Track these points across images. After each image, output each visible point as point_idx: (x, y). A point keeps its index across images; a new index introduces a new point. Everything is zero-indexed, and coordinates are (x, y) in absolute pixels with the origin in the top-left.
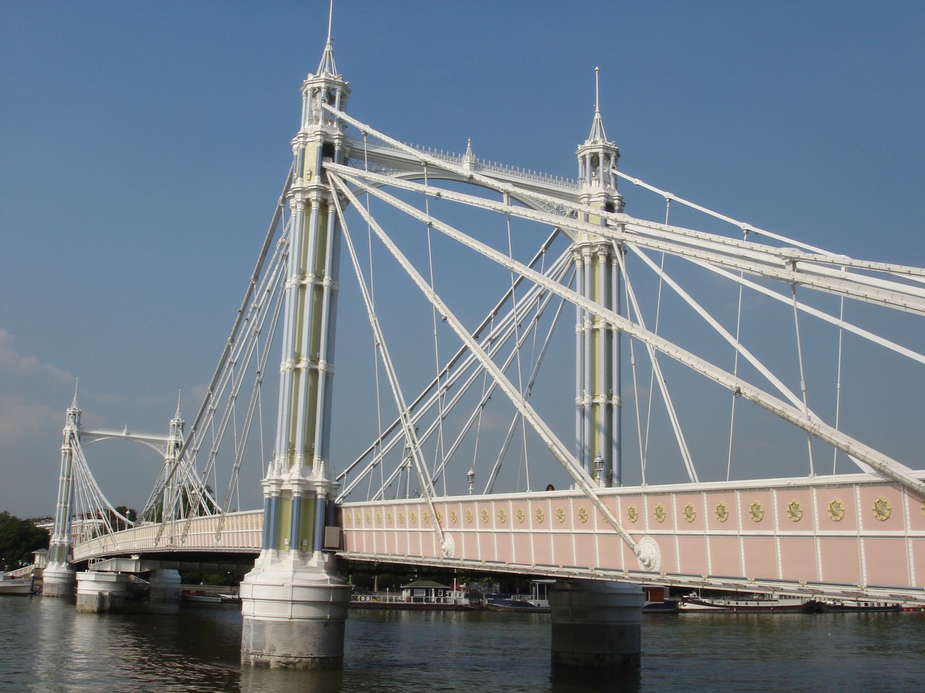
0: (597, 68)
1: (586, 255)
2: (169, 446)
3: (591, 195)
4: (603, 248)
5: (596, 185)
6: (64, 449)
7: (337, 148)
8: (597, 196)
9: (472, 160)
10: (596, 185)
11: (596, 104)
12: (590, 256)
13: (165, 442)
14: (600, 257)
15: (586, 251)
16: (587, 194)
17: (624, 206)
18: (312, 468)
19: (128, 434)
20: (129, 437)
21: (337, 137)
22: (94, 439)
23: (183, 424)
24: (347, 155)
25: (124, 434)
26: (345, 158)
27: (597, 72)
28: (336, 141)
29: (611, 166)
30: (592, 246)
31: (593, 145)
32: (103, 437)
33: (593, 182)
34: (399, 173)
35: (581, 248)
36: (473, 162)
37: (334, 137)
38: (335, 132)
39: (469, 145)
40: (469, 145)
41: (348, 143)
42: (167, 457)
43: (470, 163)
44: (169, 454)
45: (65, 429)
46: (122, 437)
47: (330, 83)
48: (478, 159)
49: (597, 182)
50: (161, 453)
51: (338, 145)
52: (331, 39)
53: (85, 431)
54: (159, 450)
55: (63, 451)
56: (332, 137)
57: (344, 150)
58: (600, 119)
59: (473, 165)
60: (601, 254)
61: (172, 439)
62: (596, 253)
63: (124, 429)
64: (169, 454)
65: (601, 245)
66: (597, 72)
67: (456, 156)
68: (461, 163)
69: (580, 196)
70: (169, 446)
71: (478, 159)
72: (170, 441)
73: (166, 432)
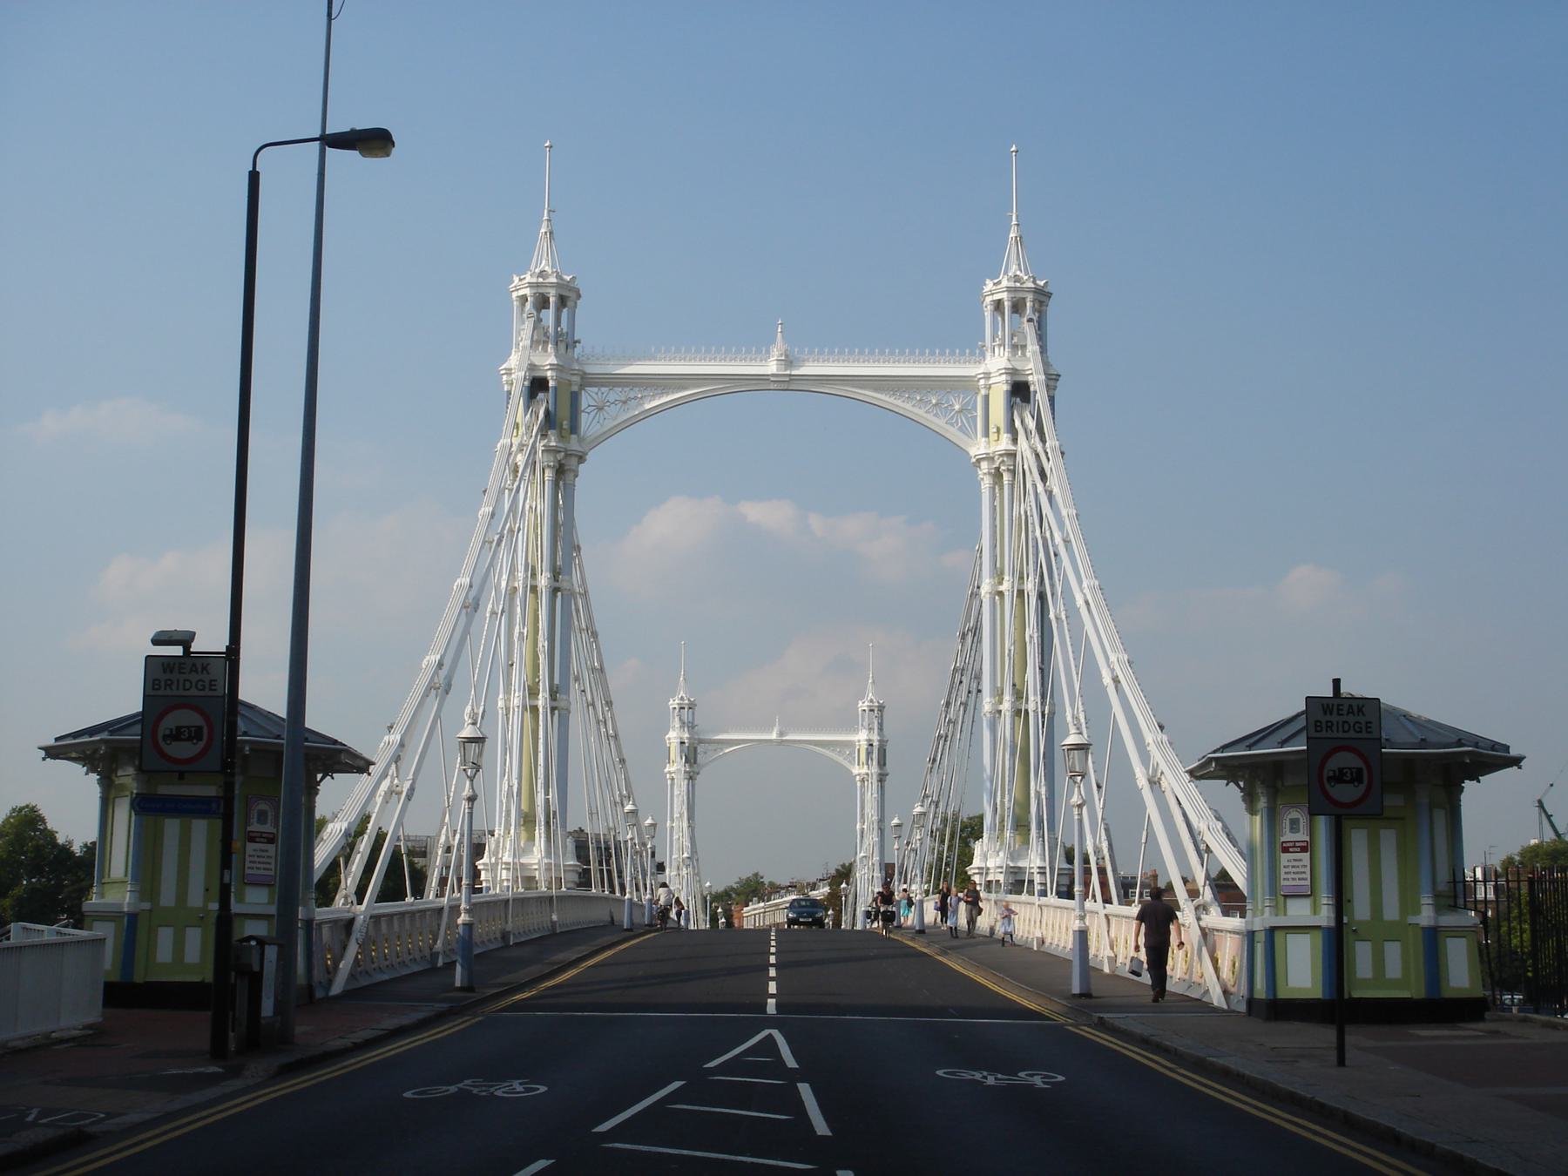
0: (1014, 148)
1: (985, 474)
2: (859, 750)
3: (990, 373)
4: (1005, 459)
5: (999, 355)
6: (670, 773)
7: (551, 384)
8: (997, 374)
9: (781, 355)
10: (999, 355)
11: (1012, 212)
12: (989, 473)
13: (850, 744)
14: (1004, 474)
15: (984, 465)
16: (983, 373)
17: (1058, 380)
18: (534, 845)
19: (781, 734)
20: (783, 741)
21: (548, 367)
22: (722, 749)
23: (881, 708)
24: (575, 388)
25: (774, 736)
26: (572, 393)
27: (1014, 154)
28: (549, 374)
29: (1025, 319)
30: (990, 459)
31: (994, 288)
32: (737, 745)
33: (996, 349)
34: (665, 395)
35: (979, 461)
36: (783, 358)
37: (546, 368)
38: (547, 360)
39: (779, 330)
40: (779, 330)
41: (572, 370)
42: (856, 770)
43: (777, 360)
44: (859, 764)
45: (667, 736)
46: (770, 741)
47: (538, 286)
48: (796, 350)
49: (1002, 348)
50: (846, 763)
51: (552, 379)
52: (549, 211)
53: (701, 737)
54: (840, 759)
55: (668, 776)
56: (542, 368)
57: (570, 381)
58: (1016, 237)
59: (783, 363)
60: (1004, 470)
61: (861, 737)
62: (999, 468)
63: (775, 725)
64: (859, 764)
65: (1001, 455)
66: (1014, 154)
67: (759, 351)
68: (766, 361)
69: (975, 377)
70: (859, 750)
71: (796, 350)
72: (859, 741)
73: (852, 726)
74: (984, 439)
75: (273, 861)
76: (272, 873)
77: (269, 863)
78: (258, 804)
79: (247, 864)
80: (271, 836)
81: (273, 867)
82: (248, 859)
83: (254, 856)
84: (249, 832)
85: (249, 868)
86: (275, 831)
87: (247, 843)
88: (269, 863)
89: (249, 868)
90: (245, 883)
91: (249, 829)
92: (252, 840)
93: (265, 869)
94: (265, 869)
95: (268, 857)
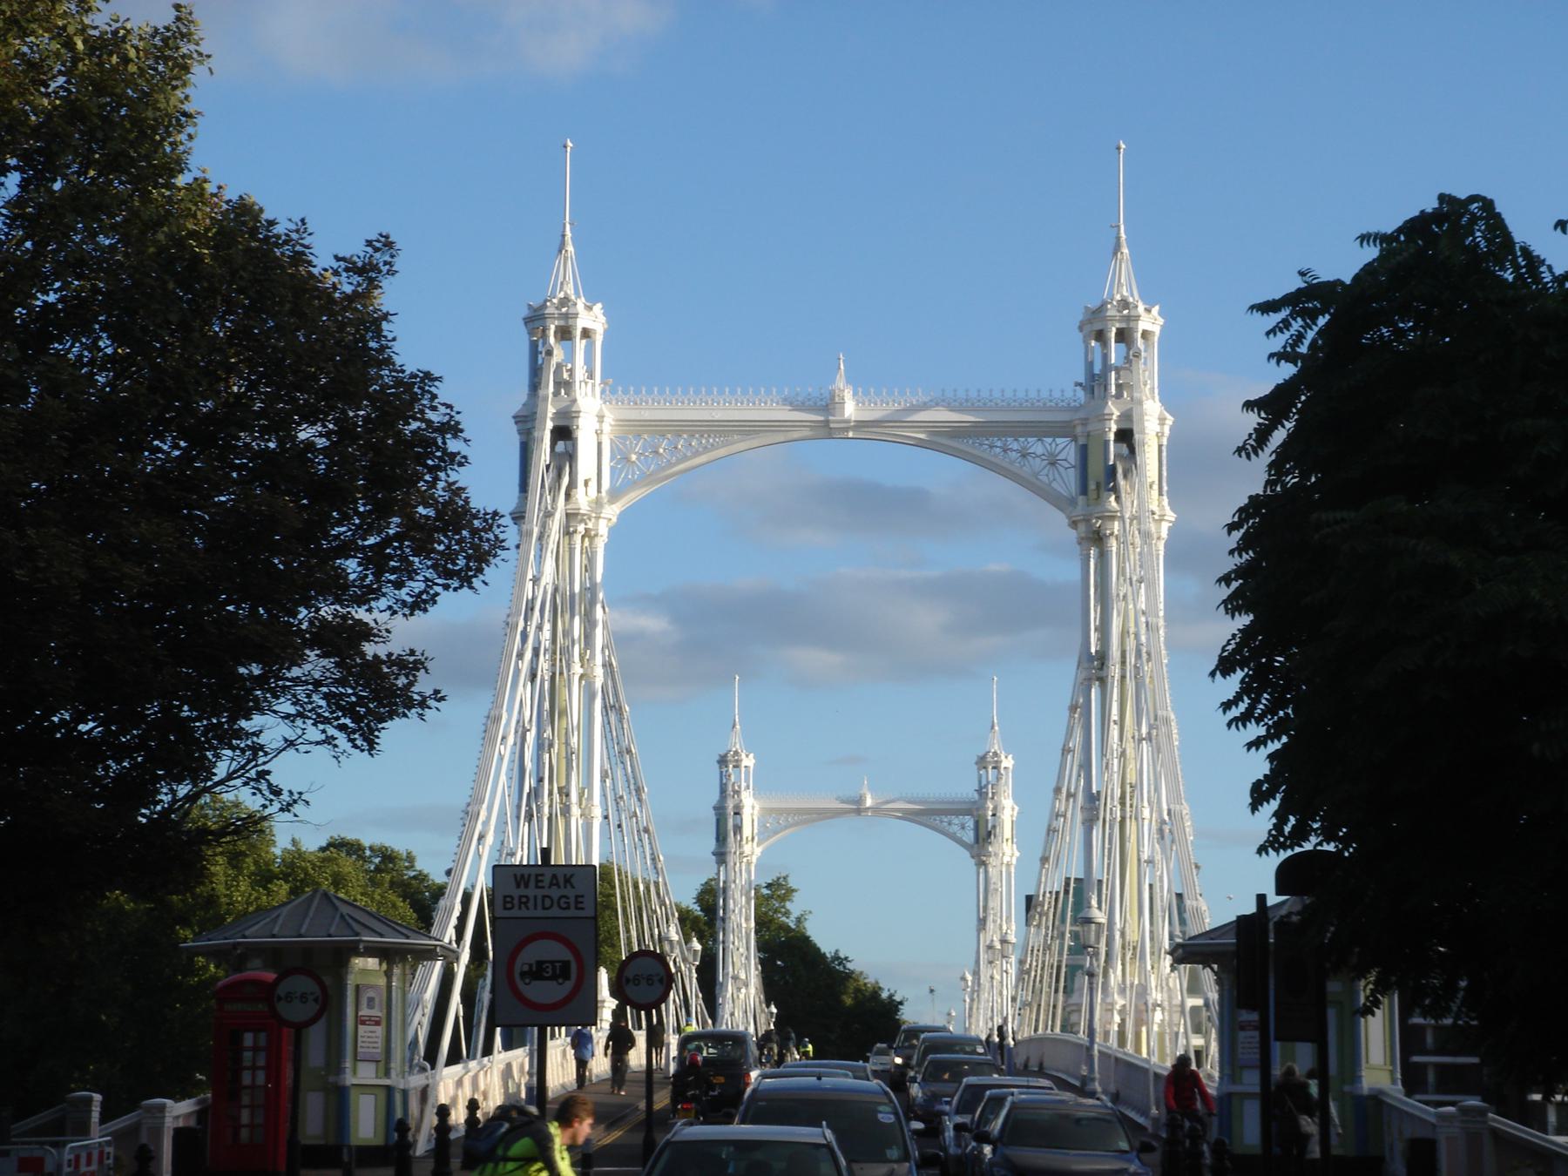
74: (1081, 497)
75: (379, 1040)
76: (379, 1051)
77: (376, 1042)
79: (359, 1044)
81: (379, 1045)
86: (380, 1014)
88: (376, 1042)
92: (363, 1023)
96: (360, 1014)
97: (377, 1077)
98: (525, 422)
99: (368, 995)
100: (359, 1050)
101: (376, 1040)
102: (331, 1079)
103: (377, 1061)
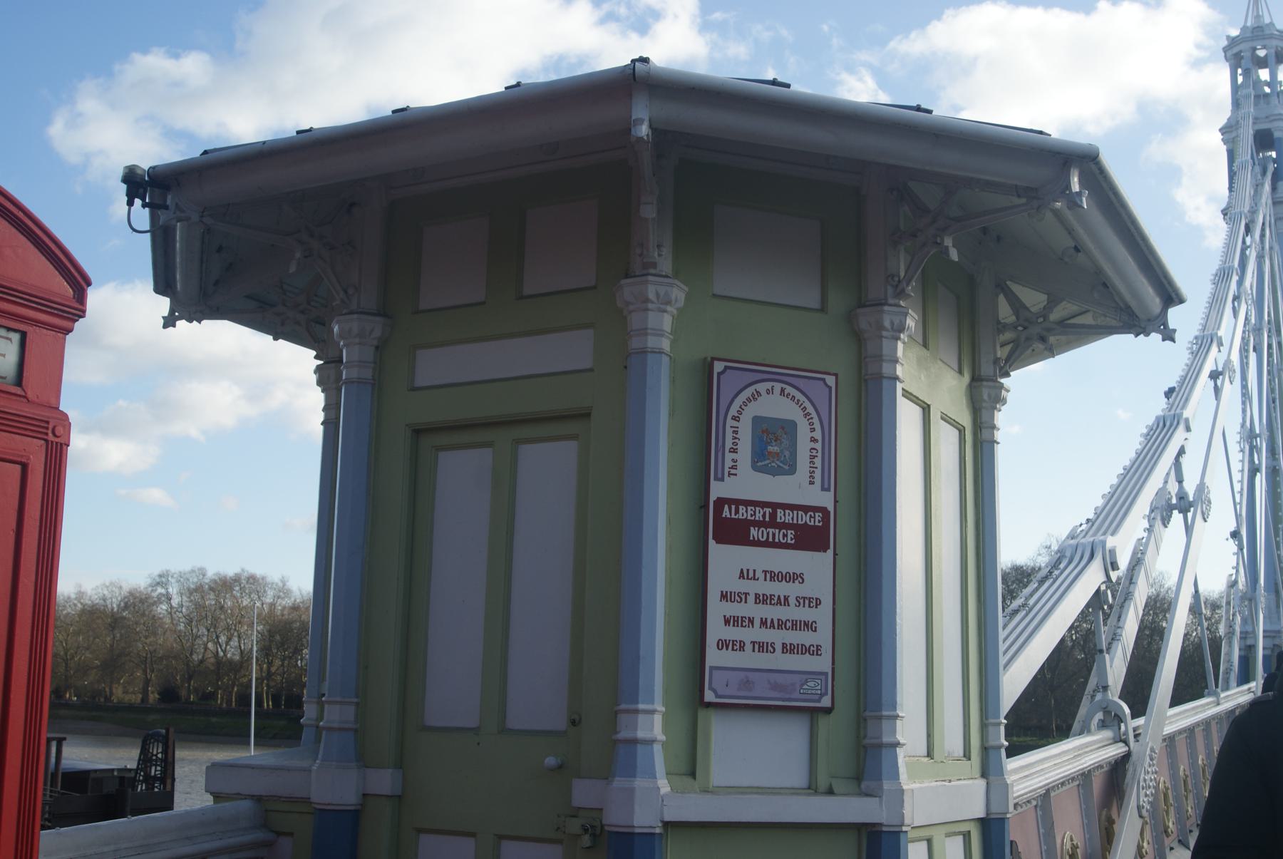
75: (823, 616)
76: (822, 663)
77: (809, 626)
78: (756, 396)
79: (716, 630)
80: (817, 520)
81: (823, 637)
82: (716, 610)
83: (742, 597)
84: (721, 502)
85: (723, 644)
86: (826, 500)
87: (712, 542)
88: (809, 626)
89: (723, 644)
90: (709, 705)
91: (718, 490)
92: (735, 533)
93: (788, 649)
94: (788, 649)
95: (801, 601)
96: (718, 490)
97: (812, 788)
98: (1231, 132)
99: (753, 410)
100: (714, 657)
101: (804, 614)
102: (584, 793)
103: (814, 713)
